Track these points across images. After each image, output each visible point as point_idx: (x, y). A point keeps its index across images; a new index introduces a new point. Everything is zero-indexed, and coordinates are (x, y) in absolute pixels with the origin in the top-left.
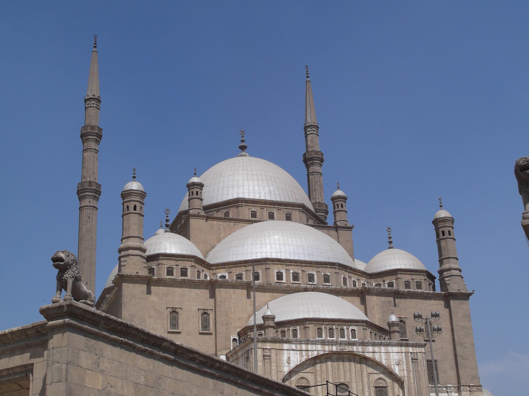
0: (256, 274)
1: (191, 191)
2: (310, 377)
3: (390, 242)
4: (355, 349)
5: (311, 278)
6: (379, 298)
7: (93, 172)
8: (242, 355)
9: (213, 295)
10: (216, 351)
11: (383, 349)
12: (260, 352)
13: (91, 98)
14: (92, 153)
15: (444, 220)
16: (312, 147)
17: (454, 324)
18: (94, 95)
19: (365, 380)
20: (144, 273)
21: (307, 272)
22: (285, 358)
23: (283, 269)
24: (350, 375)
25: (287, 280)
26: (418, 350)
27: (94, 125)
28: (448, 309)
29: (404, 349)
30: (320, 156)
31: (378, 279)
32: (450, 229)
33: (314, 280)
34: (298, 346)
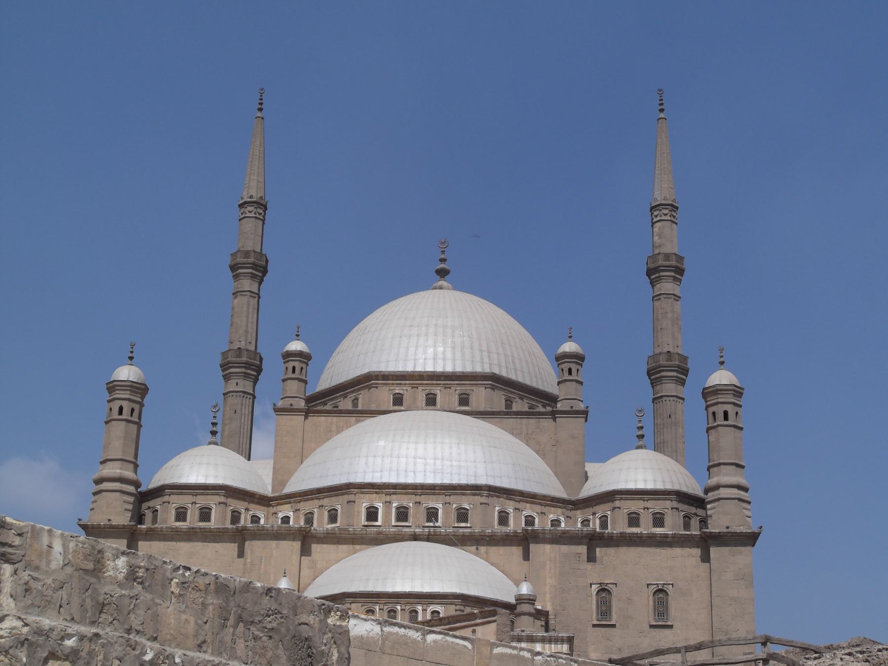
0: (333, 512)
3: (641, 437)
5: (432, 514)
6: (556, 547)
7: (247, 332)
9: (241, 554)
13: (245, 203)
14: (245, 299)
16: (660, 246)
17: (714, 594)
18: (251, 197)
21: (425, 505)
23: (380, 501)
25: (384, 521)
26: (554, 648)
27: (249, 249)
28: (707, 564)
30: (674, 263)
31: (586, 510)
33: (437, 520)
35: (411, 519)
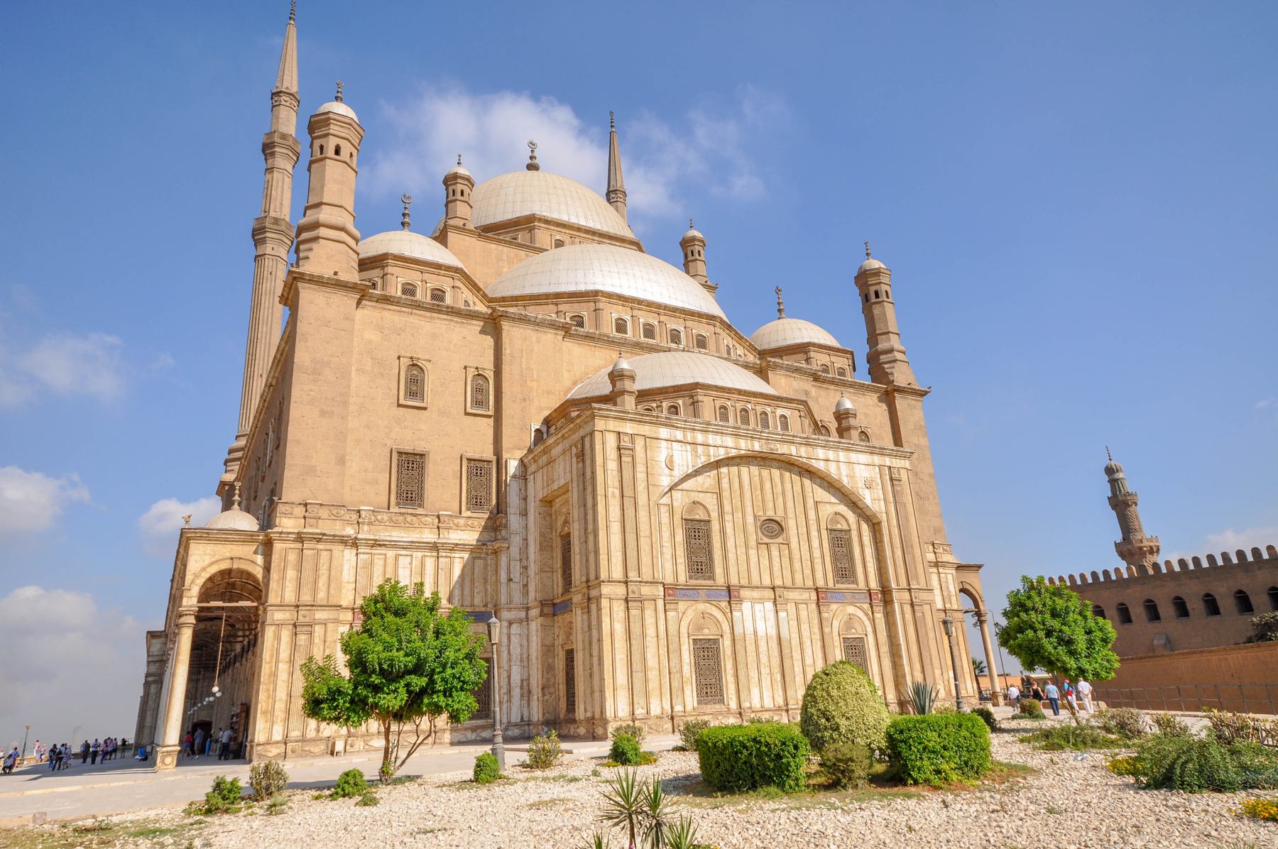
1: (451, 189)
2: (710, 501)
4: (793, 450)
5: (675, 337)
8: (564, 452)
10: (498, 452)
11: (842, 455)
12: (611, 440)
15: (877, 273)
19: (812, 514)
20: (353, 277)
22: (662, 456)
24: (785, 504)
29: (877, 459)
32: (888, 288)
34: (689, 435)
35: (657, 336)
